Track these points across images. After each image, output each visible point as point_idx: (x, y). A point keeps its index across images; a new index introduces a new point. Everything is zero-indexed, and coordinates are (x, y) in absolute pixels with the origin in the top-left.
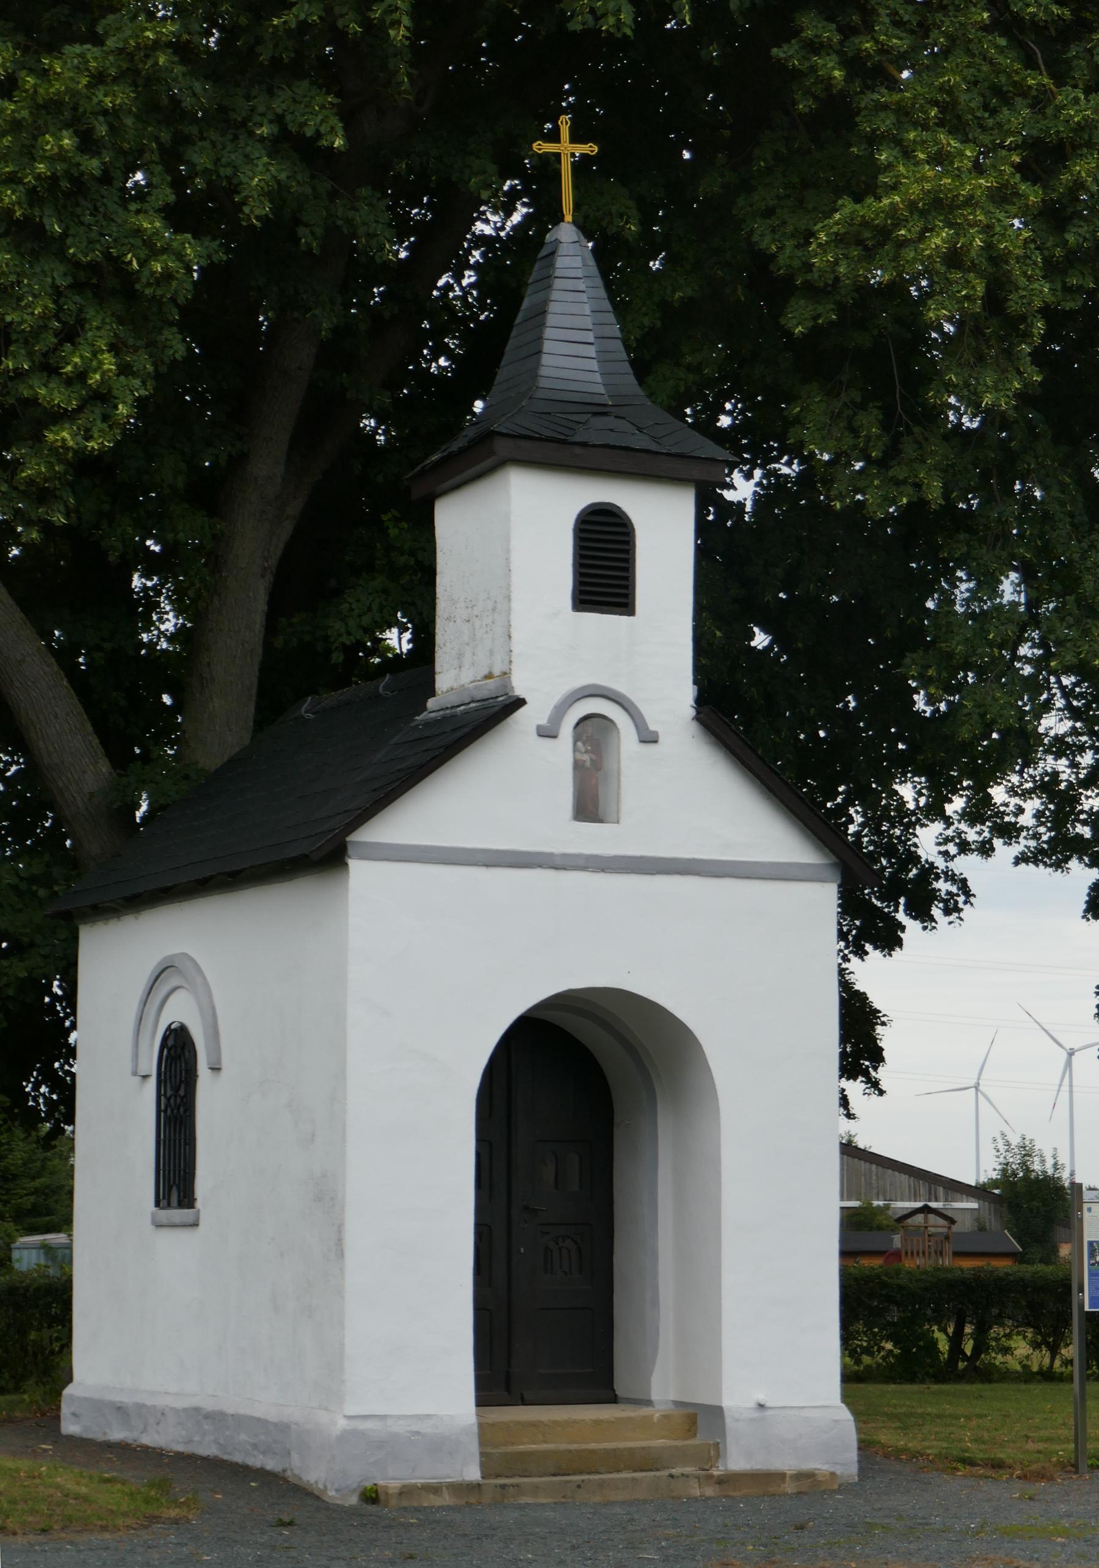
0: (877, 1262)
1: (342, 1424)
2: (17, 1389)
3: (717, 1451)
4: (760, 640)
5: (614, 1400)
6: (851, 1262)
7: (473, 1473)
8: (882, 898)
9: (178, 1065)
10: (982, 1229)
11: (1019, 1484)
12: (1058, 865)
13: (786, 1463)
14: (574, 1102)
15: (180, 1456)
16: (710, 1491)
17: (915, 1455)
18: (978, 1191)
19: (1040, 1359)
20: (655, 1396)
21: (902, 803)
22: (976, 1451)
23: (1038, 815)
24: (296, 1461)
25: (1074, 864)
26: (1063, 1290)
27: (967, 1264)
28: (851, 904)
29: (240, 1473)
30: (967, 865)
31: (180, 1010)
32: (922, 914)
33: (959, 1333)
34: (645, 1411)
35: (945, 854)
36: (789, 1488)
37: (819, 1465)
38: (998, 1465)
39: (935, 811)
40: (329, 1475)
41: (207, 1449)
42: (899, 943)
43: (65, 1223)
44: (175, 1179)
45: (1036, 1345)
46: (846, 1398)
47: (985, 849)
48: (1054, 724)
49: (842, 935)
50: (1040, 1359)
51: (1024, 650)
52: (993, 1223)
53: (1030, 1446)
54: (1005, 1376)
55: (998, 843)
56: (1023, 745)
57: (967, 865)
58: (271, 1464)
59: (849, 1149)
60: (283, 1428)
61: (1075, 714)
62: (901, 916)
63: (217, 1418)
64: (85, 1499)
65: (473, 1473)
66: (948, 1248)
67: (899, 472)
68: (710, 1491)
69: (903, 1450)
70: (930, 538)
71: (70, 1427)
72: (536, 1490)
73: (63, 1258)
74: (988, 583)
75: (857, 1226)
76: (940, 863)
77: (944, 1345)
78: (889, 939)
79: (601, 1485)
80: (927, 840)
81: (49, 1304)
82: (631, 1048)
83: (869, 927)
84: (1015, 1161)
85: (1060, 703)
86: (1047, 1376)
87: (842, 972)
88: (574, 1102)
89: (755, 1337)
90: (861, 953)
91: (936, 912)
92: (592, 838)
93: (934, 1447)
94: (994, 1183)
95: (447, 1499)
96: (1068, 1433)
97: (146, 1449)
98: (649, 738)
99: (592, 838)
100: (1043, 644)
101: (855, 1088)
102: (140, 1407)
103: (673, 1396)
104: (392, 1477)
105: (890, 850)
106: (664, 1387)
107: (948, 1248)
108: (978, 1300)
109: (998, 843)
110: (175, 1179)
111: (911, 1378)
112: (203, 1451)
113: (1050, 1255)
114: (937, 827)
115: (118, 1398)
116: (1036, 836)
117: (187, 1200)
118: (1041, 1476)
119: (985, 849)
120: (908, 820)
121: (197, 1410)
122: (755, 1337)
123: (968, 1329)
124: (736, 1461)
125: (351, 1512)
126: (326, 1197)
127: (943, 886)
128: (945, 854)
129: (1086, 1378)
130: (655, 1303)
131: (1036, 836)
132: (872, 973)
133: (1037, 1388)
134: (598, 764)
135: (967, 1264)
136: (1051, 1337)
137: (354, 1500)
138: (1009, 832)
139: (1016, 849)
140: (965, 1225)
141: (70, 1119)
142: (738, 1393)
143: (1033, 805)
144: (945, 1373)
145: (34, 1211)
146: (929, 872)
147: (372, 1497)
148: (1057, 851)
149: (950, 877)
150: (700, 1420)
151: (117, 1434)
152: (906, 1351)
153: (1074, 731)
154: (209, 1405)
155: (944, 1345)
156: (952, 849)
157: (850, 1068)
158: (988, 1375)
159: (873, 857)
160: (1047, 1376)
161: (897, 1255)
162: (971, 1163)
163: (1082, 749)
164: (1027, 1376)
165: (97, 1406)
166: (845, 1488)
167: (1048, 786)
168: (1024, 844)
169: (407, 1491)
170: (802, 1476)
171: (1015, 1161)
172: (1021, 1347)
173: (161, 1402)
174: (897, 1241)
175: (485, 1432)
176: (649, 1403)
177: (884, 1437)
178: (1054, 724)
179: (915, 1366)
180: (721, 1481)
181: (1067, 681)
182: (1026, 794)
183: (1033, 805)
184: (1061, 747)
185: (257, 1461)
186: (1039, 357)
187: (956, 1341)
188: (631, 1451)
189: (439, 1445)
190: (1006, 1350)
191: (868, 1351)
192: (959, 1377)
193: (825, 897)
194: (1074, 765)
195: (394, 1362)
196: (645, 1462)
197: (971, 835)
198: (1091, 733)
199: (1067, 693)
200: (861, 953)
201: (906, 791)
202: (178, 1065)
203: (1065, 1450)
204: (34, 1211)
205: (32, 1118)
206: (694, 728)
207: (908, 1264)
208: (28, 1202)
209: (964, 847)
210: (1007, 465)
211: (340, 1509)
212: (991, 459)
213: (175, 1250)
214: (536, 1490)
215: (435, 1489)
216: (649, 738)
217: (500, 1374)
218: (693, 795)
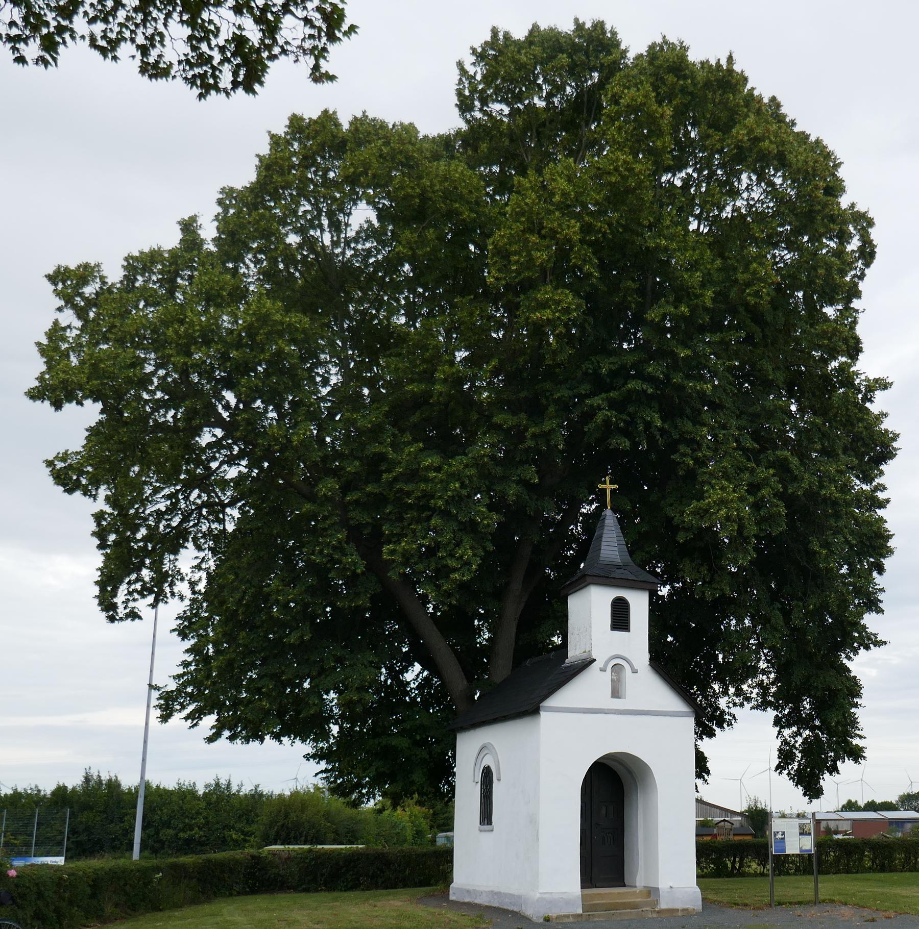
0: (709, 838)
1: (538, 895)
2: (436, 885)
3: (657, 902)
4: (670, 639)
5: (625, 886)
6: (700, 839)
7: (580, 911)
8: (709, 721)
9: (487, 777)
10: (742, 826)
11: (753, 911)
12: (764, 710)
13: (679, 906)
14: (611, 789)
15: (487, 906)
16: (655, 915)
17: (719, 902)
18: (741, 814)
19: (760, 869)
20: (637, 885)
21: (715, 690)
22: (739, 901)
23: (757, 694)
24: (523, 908)
25: (769, 709)
26: (766, 846)
27: (737, 838)
28: (699, 723)
29: (506, 912)
30: (735, 711)
31: (488, 761)
32: (720, 726)
33: (734, 860)
34: (634, 889)
35: (728, 707)
36: (680, 914)
37: (689, 906)
38: (746, 905)
39: (725, 693)
40: (534, 912)
41: (495, 904)
42: (715, 735)
43: (452, 830)
44: (486, 816)
45: (759, 865)
46: (698, 884)
47: (742, 705)
48: (762, 665)
49: (696, 733)
50: (760, 869)
51: (752, 641)
52: (745, 824)
53: (756, 898)
54: (749, 875)
55: (745, 703)
56: (753, 671)
57: (735, 711)
58: (515, 909)
59: (699, 801)
60: (519, 897)
61: (768, 661)
62: (714, 727)
63: (498, 894)
64: (456, 922)
65: (580, 911)
66: (731, 833)
67: (715, 586)
68: (655, 915)
69: (715, 901)
70: (724, 606)
71: (452, 897)
72: (600, 916)
73: (450, 840)
74: (740, 621)
75: (703, 828)
76: (727, 710)
77: (730, 865)
78: (711, 734)
79: (620, 914)
80: (723, 702)
81: (447, 856)
82: (630, 772)
83: (704, 731)
84: (752, 804)
85: (763, 658)
86: (762, 875)
87: (696, 745)
88: (611, 789)
89: (668, 862)
90: (702, 739)
91: (725, 725)
92: (617, 704)
93: (726, 899)
94: (746, 811)
95: (571, 920)
96: (768, 894)
97: (476, 904)
98: (635, 671)
99: (617, 704)
100: (758, 639)
101: (699, 782)
102: (474, 890)
103: (643, 884)
104: (554, 913)
105: (711, 706)
106: (640, 879)
107: (731, 833)
108: (740, 850)
109: (745, 703)
110: (486, 816)
111: (719, 876)
112: (494, 905)
113: (763, 835)
114: (726, 698)
115: (468, 888)
116: (757, 700)
117: (490, 822)
118: (759, 908)
119: (742, 705)
120: (716, 696)
121: (492, 891)
122: (668, 862)
123: (737, 859)
124: (663, 905)
125: (540, 925)
126: (533, 821)
127: (727, 717)
128: (728, 707)
129: (774, 875)
130: (638, 854)
131: (757, 700)
132: (706, 745)
133: (759, 879)
134: (619, 680)
135: (737, 838)
136: (763, 861)
137: (542, 920)
138: (748, 699)
139: (751, 705)
140: (737, 825)
141: (453, 796)
142: (663, 884)
143: (756, 691)
144: (730, 875)
145: (444, 825)
146: (723, 712)
147: (547, 919)
148: (764, 705)
149: (730, 714)
150: (652, 892)
151: (467, 900)
152: (718, 867)
153: (768, 667)
154: (496, 890)
155: (730, 865)
156: (731, 705)
157: (699, 775)
158: (743, 875)
159: (705, 708)
160: (762, 875)
161: (715, 836)
162: (739, 806)
163: (770, 672)
164: (756, 875)
165: (461, 890)
166: (698, 914)
167: (760, 685)
168: (753, 703)
169: (558, 917)
170: (683, 910)
171: (752, 804)
172: (754, 865)
173: (481, 889)
174: (715, 831)
175: (583, 897)
176: (635, 887)
177: (710, 897)
178: (762, 665)
179: (720, 872)
180: (658, 912)
181: (765, 651)
182: (754, 687)
183: (756, 691)
184: (764, 672)
185: (511, 908)
186: (756, 549)
187: (733, 863)
188: (630, 903)
189: (568, 902)
190: (749, 866)
191: (706, 868)
192: (734, 876)
193: (690, 722)
194: (768, 678)
195: (553, 870)
196: (634, 906)
197: (737, 701)
198: (773, 668)
199: (765, 655)
200: (702, 739)
201: (716, 687)
202: (487, 777)
203: (767, 900)
204: (444, 825)
205: (443, 795)
206: (649, 668)
207: (719, 839)
208: (441, 822)
209: (735, 705)
210: (746, 583)
211: (537, 924)
212: (741, 582)
213: (486, 839)
214: (600, 916)
215: (567, 916)
216: (635, 671)
217: (589, 878)
218: (650, 690)
